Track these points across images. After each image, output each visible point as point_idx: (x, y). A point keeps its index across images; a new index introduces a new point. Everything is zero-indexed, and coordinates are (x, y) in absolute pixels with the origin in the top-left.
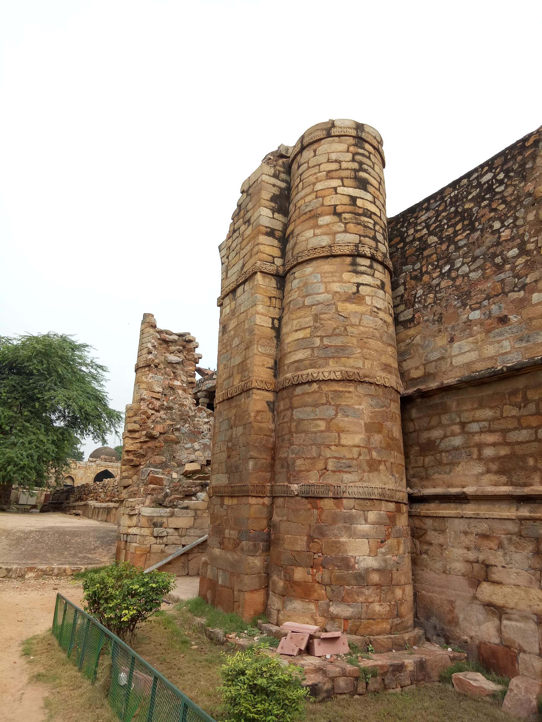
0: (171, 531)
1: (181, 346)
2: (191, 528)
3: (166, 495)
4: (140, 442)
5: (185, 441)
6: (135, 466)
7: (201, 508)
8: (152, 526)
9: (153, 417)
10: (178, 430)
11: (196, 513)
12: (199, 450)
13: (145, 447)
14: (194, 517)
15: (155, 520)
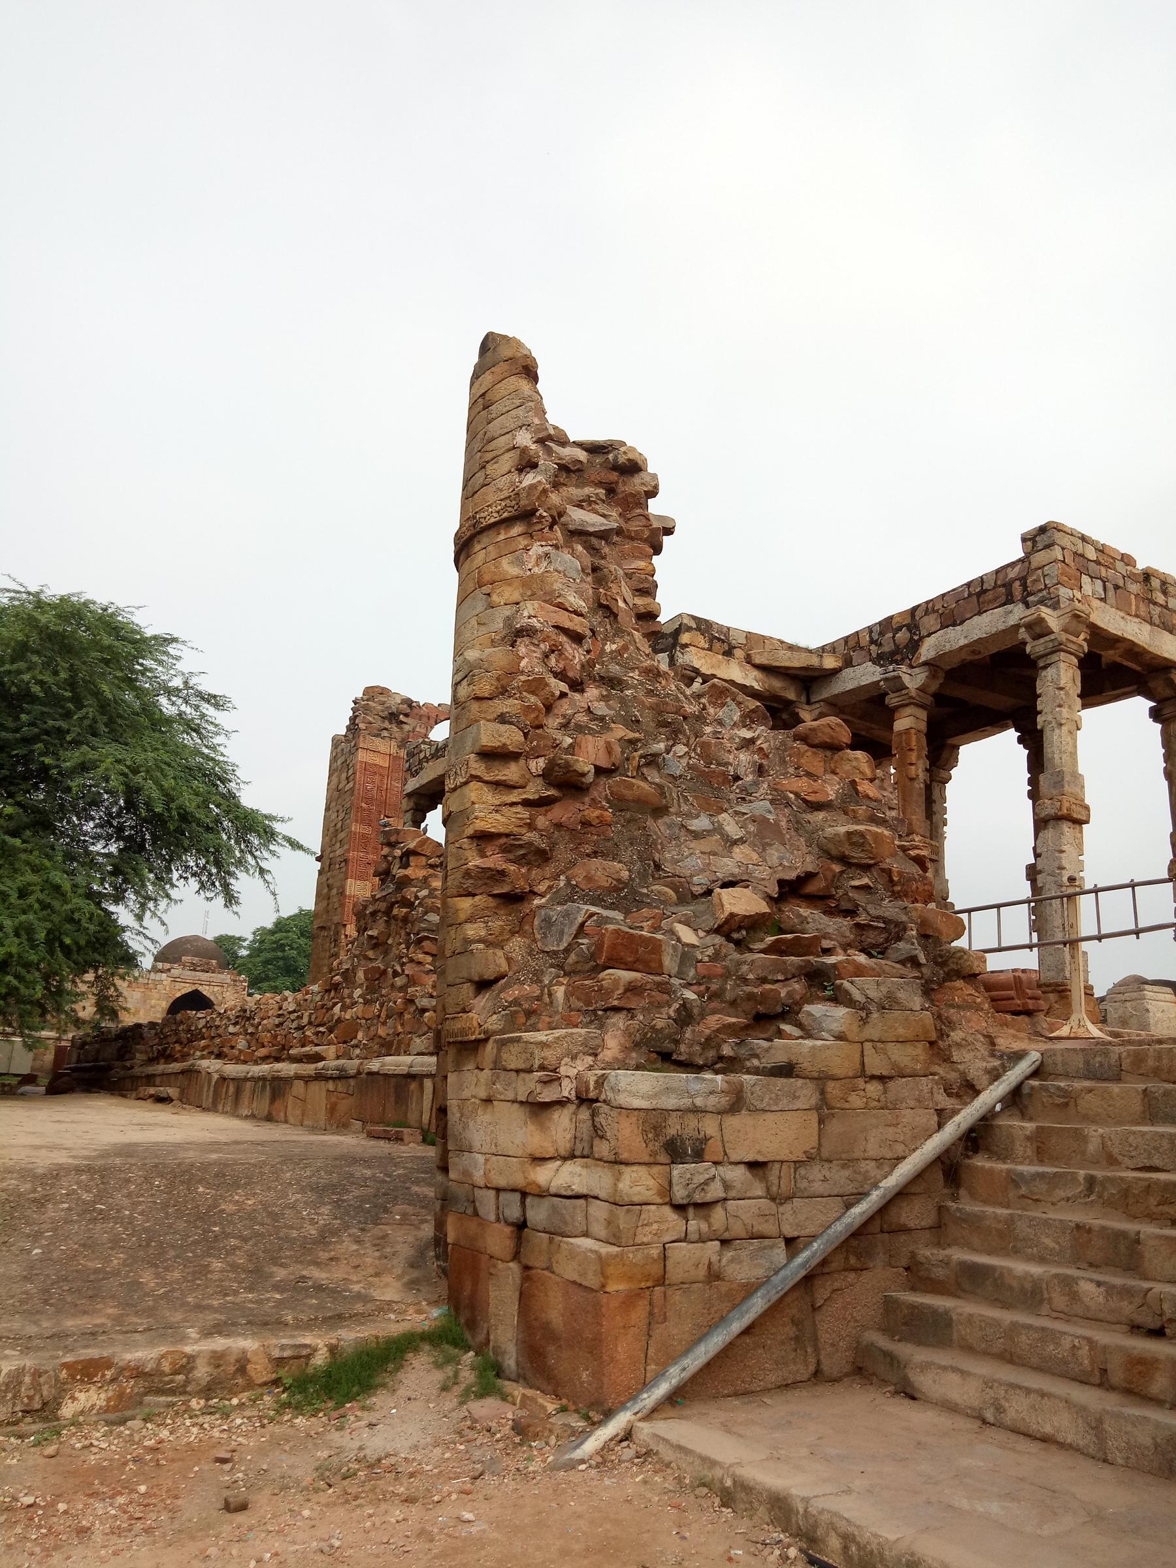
0: (737, 1174)
1: (600, 484)
2: (810, 1159)
3: (686, 1016)
4: (526, 803)
5: (685, 808)
6: (513, 899)
7: (837, 1071)
8: (663, 1158)
9: (565, 707)
10: (653, 760)
11: (823, 1092)
12: (741, 841)
13: (542, 822)
14: (818, 1108)
15: (673, 1129)
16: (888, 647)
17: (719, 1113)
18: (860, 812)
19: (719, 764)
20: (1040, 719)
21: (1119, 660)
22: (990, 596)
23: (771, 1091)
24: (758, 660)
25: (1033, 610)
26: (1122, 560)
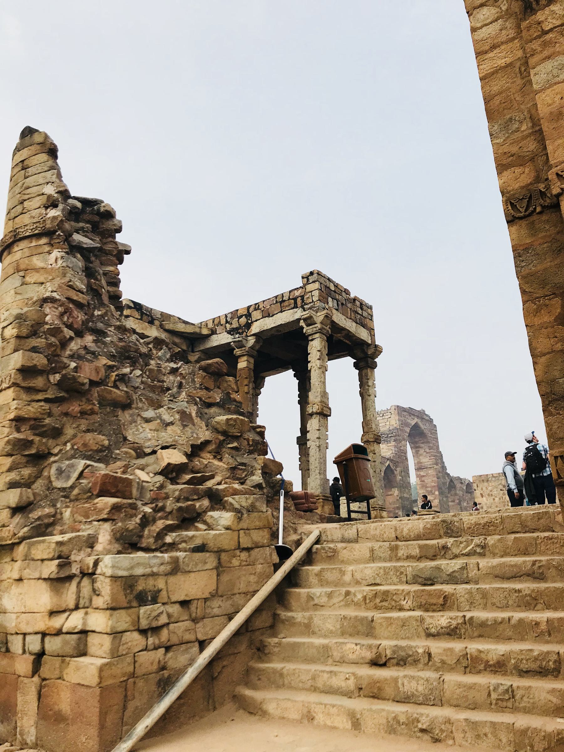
0: (175, 609)
1: (88, 222)
2: (214, 595)
3: (146, 521)
4: (46, 400)
5: (140, 405)
7: (226, 547)
8: (135, 604)
9: (74, 346)
10: (123, 378)
11: (219, 559)
12: (172, 423)
14: (217, 568)
15: (141, 586)
16: (235, 325)
17: (166, 575)
18: (232, 408)
19: (159, 381)
20: (309, 365)
21: (342, 338)
22: (286, 303)
23: (193, 561)
24: (167, 327)
25: (307, 312)
26: (345, 292)
